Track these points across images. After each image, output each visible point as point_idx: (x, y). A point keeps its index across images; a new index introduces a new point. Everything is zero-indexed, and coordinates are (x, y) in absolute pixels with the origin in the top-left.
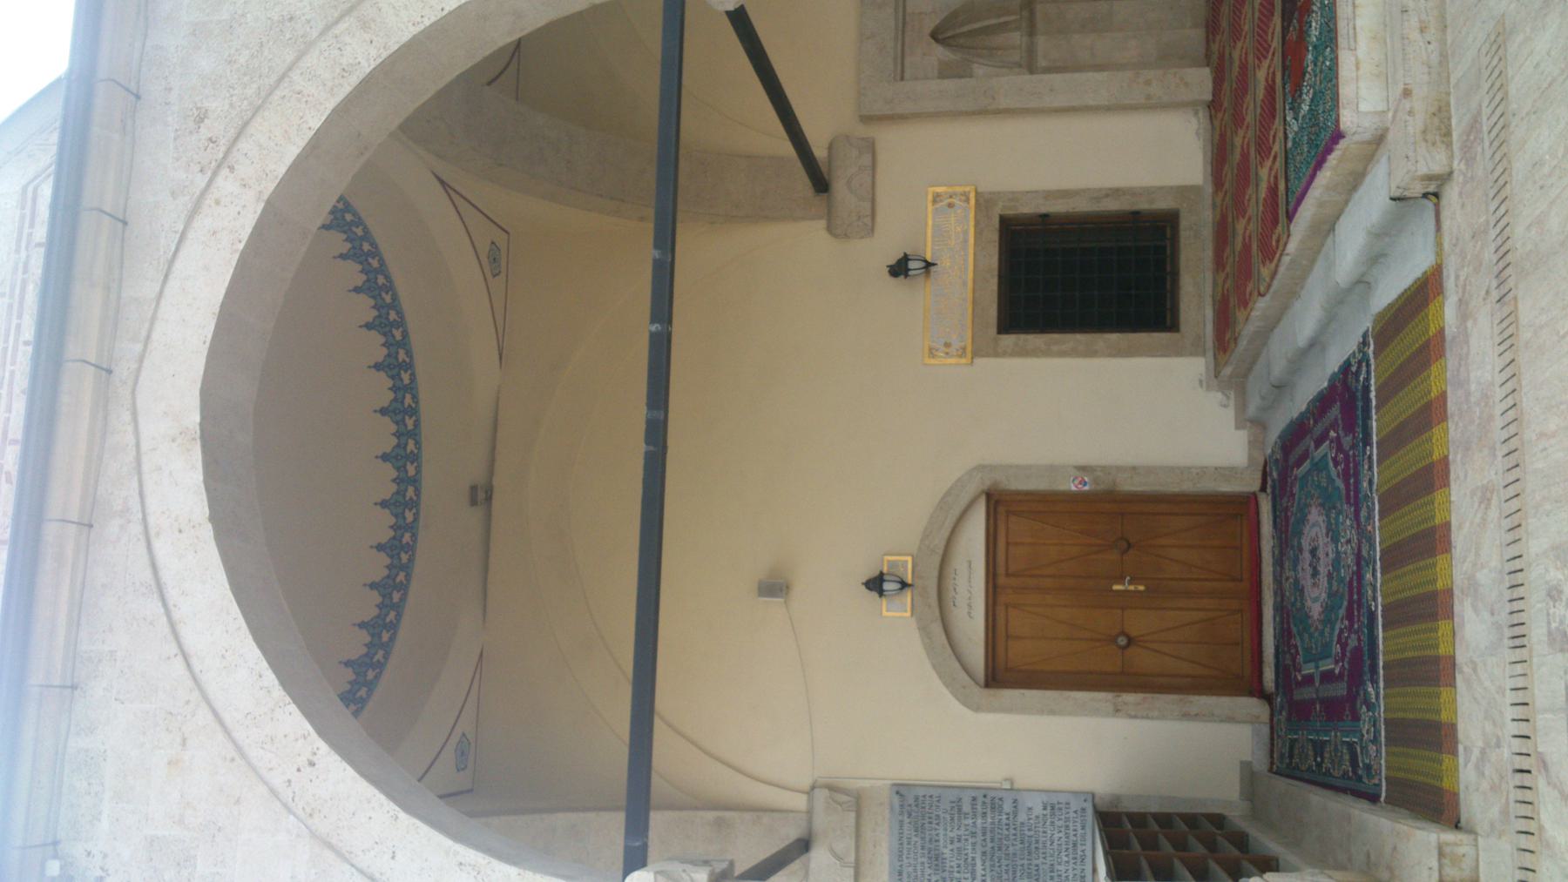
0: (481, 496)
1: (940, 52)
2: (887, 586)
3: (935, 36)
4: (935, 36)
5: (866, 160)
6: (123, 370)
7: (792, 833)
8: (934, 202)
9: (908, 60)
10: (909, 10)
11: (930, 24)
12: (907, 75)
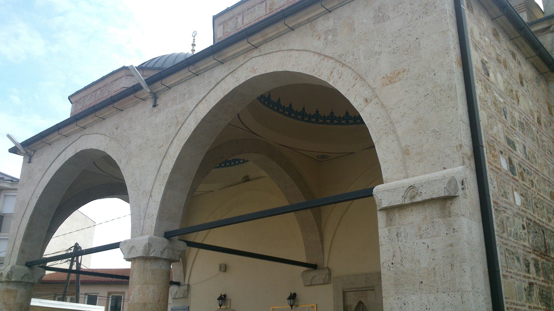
0: (247, 179)
1: (355, 305)
2: (221, 301)
3: (360, 303)
4: (360, 303)
5: (322, 282)
6: (86, 131)
7: (181, 281)
8: (312, 307)
9: (352, 293)
10: (368, 292)
11: (363, 300)
12: (348, 293)
